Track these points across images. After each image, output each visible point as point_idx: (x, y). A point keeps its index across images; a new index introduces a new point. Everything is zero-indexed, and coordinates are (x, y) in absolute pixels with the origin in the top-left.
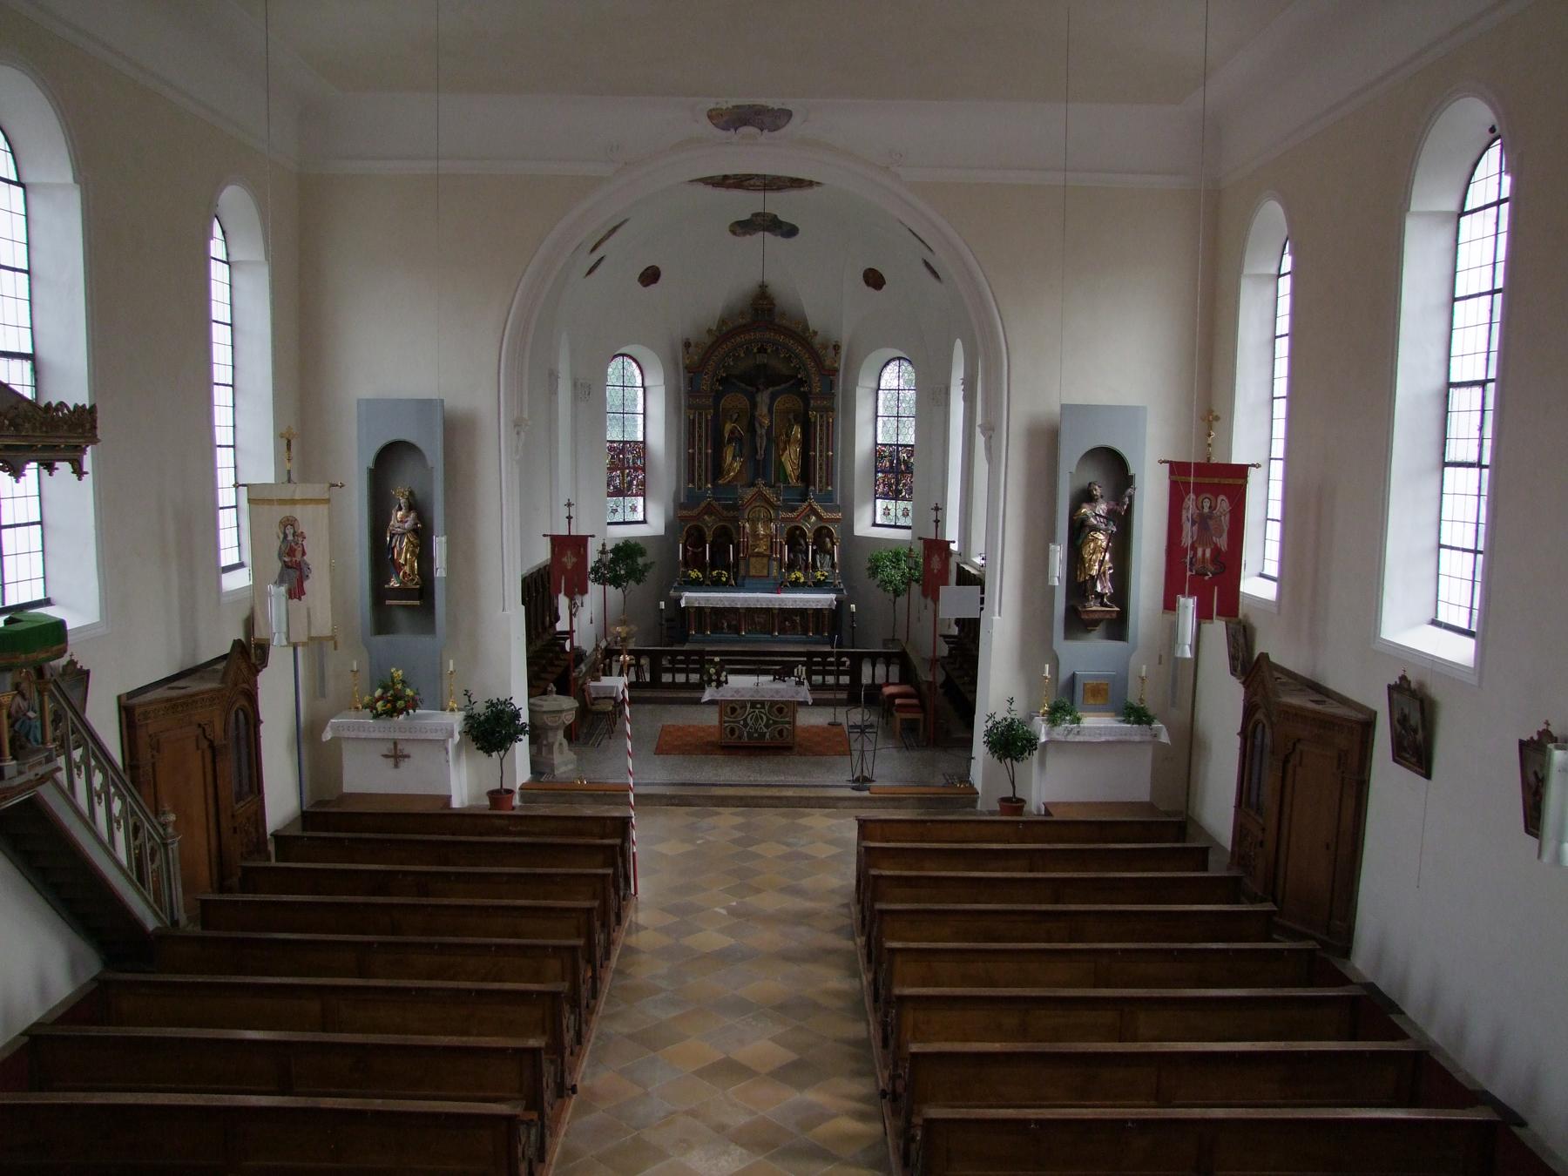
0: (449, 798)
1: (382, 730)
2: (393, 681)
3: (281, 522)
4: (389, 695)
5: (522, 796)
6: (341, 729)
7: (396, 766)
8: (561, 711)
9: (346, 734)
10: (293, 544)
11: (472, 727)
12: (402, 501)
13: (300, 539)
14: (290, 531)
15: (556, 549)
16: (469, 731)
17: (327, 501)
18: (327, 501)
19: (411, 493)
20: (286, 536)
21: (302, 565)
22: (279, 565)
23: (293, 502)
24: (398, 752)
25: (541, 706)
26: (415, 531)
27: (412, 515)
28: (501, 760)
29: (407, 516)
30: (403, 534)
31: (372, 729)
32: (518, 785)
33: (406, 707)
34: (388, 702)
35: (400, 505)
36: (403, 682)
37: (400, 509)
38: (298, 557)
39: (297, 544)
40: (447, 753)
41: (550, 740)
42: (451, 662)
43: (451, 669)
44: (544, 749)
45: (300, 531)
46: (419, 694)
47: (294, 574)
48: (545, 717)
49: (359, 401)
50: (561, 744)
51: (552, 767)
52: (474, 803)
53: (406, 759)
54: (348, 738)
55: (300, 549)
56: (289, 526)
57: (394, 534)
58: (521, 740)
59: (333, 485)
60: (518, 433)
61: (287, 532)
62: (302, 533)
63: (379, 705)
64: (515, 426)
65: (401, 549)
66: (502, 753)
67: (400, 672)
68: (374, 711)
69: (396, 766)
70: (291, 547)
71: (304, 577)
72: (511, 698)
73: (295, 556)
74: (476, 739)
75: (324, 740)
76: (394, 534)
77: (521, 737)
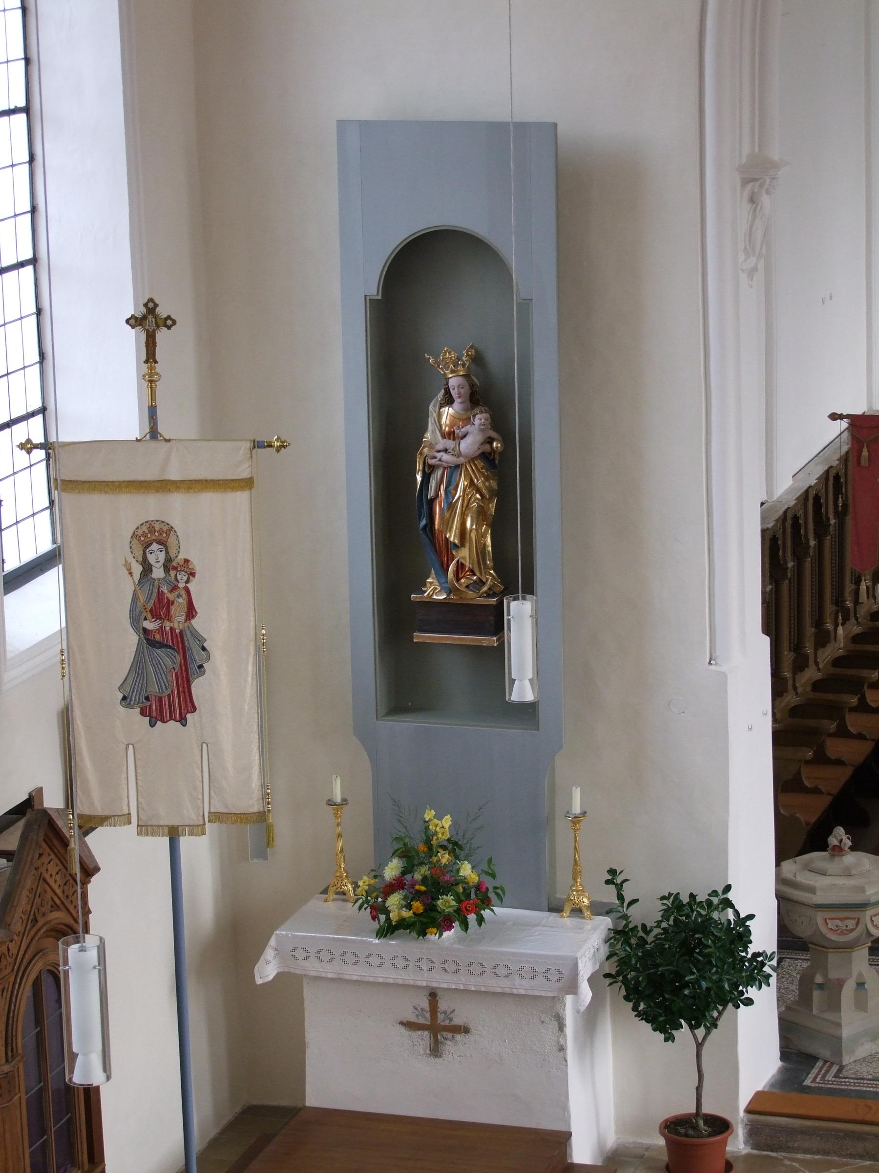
0: (562, 1139)
1: (400, 963)
2: (428, 842)
4: (418, 876)
5: (754, 1133)
6: (300, 954)
7: (435, 1051)
8: (863, 906)
9: (313, 967)
10: (165, 589)
11: (623, 963)
12: (454, 382)
13: (182, 577)
14: (157, 557)
15: (865, 453)
16: (618, 973)
17: (247, 484)
18: (247, 484)
19: (478, 359)
20: (147, 568)
21: (188, 636)
22: (133, 639)
23: (164, 486)
24: (441, 1017)
25: (812, 890)
26: (487, 458)
27: (480, 419)
28: (699, 1046)
29: (467, 421)
30: (457, 467)
31: (375, 961)
32: (744, 1099)
33: (458, 911)
34: (418, 895)
35: (448, 392)
36: (454, 846)
37: (449, 401)
38: (178, 620)
39: (175, 588)
40: (561, 1027)
41: (833, 974)
42: (577, 794)
43: (577, 809)
44: (816, 994)
45: (181, 556)
46: (493, 876)
47: (168, 660)
48: (820, 917)
49: (342, 124)
50: (861, 985)
51: (836, 1044)
52: (630, 1139)
53: (458, 1037)
54: (317, 979)
56: (155, 546)
57: (433, 468)
58: (749, 1002)
59: (258, 445)
60: (752, 200)
61: (151, 559)
62: (187, 561)
63: (394, 900)
64: (745, 182)
65: (451, 506)
66: (701, 1032)
67: (447, 822)
68: (383, 917)
69: (435, 1051)
70: (160, 594)
71: (193, 667)
72: (728, 888)
73: (168, 617)
74: (633, 994)
75: (259, 981)
76: (433, 468)
77: (752, 992)
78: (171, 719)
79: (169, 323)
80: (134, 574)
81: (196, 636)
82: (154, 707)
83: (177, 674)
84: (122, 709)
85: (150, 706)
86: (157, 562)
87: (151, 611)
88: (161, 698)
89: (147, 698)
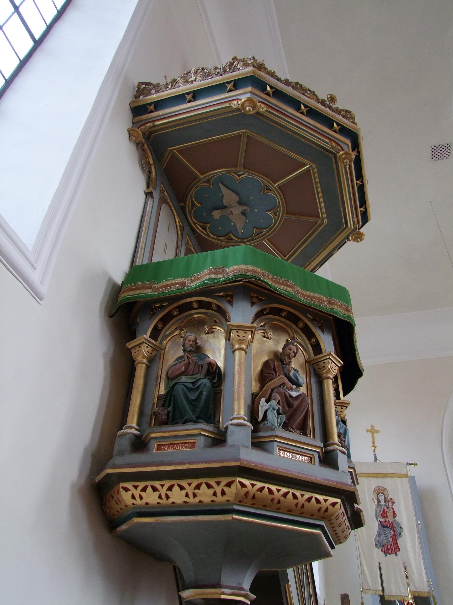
3: (374, 490)
10: (385, 508)
14: (382, 498)
20: (379, 501)
21: (394, 524)
22: (377, 524)
38: (390, 518)
39: (388, 508)
47: (390, 533)
55: (391, 511)
56: (381, 494)
61: (380, 498)
62: (391, 499)
70: (384, 509)
71: (397, 534)
73: (387, 517)
78: (392, 553)
79: (378, 432)
80: (375, 502)
81: (398, 524)
82: (386, 549)
83: (392, 537)
84: (376, 549)
85: (384, 549)
86: (382, 499)
87: (381, 515)
88: (387, 546)
89: (383, 546)
